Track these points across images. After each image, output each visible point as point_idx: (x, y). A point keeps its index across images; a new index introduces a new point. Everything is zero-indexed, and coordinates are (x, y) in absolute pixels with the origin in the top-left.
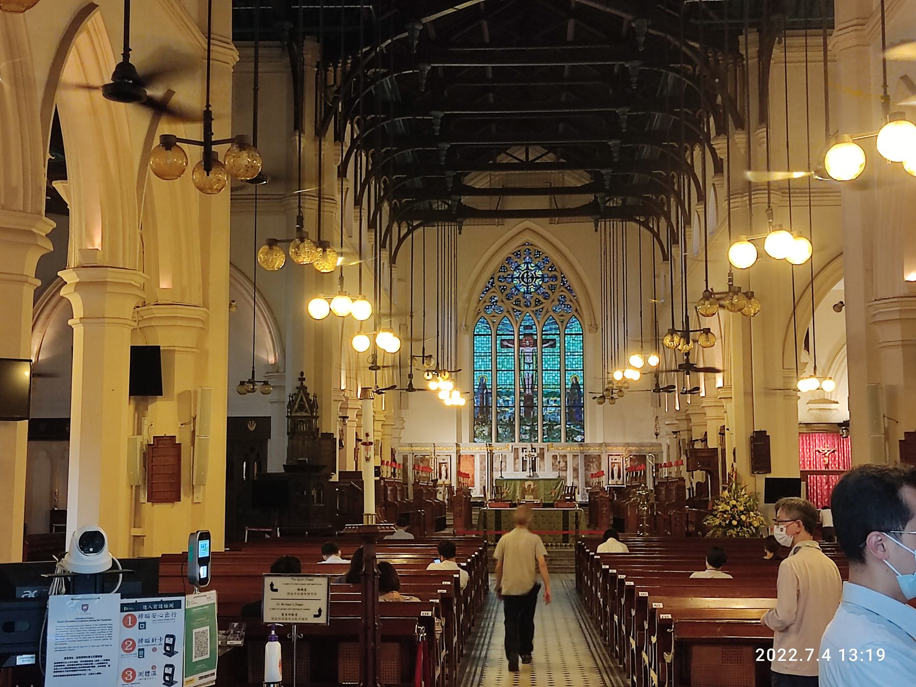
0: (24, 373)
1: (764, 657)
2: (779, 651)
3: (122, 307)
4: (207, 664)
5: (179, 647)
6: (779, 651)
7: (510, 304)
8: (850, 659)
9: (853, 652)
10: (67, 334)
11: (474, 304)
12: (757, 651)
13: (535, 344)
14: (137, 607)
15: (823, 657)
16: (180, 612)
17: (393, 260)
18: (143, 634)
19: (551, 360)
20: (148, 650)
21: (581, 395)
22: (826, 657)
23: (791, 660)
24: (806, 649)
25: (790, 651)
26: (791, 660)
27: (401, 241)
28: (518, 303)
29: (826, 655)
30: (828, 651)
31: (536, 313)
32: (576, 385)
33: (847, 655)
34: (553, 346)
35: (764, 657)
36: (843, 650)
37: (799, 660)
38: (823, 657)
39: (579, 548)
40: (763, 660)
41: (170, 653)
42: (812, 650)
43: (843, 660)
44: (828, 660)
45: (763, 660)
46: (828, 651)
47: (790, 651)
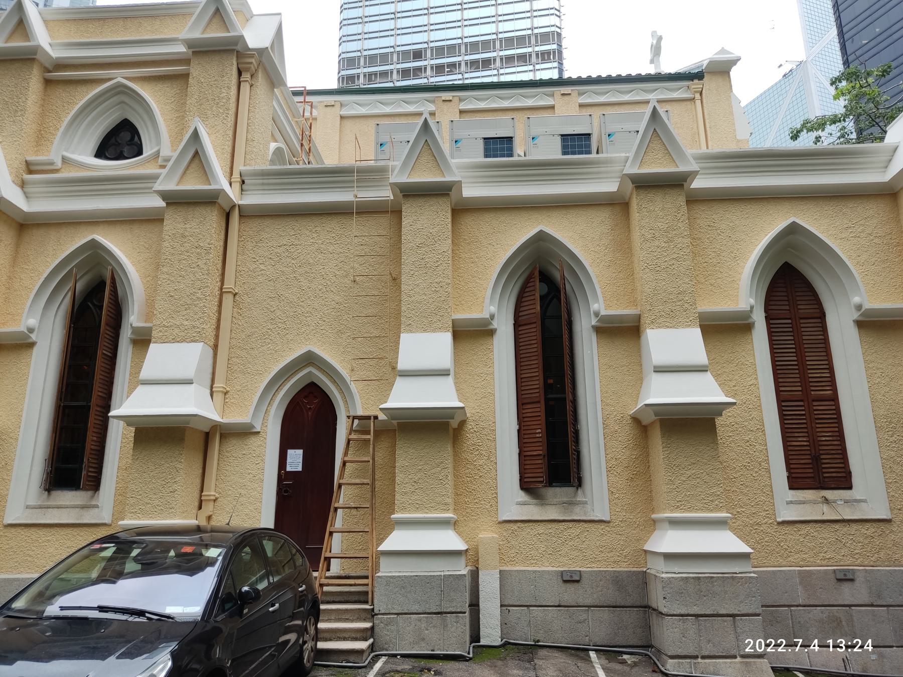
1: (754, 647)
2: (768, 642)
9: (841, 642)
12: (746, 642)
24: (795, 640)
25: (779, 642)
35: (754, 647)
37: (787, 650)
40: (753, 651)
42: (801, 640)
45: (753, 651)
47: (779, 642)
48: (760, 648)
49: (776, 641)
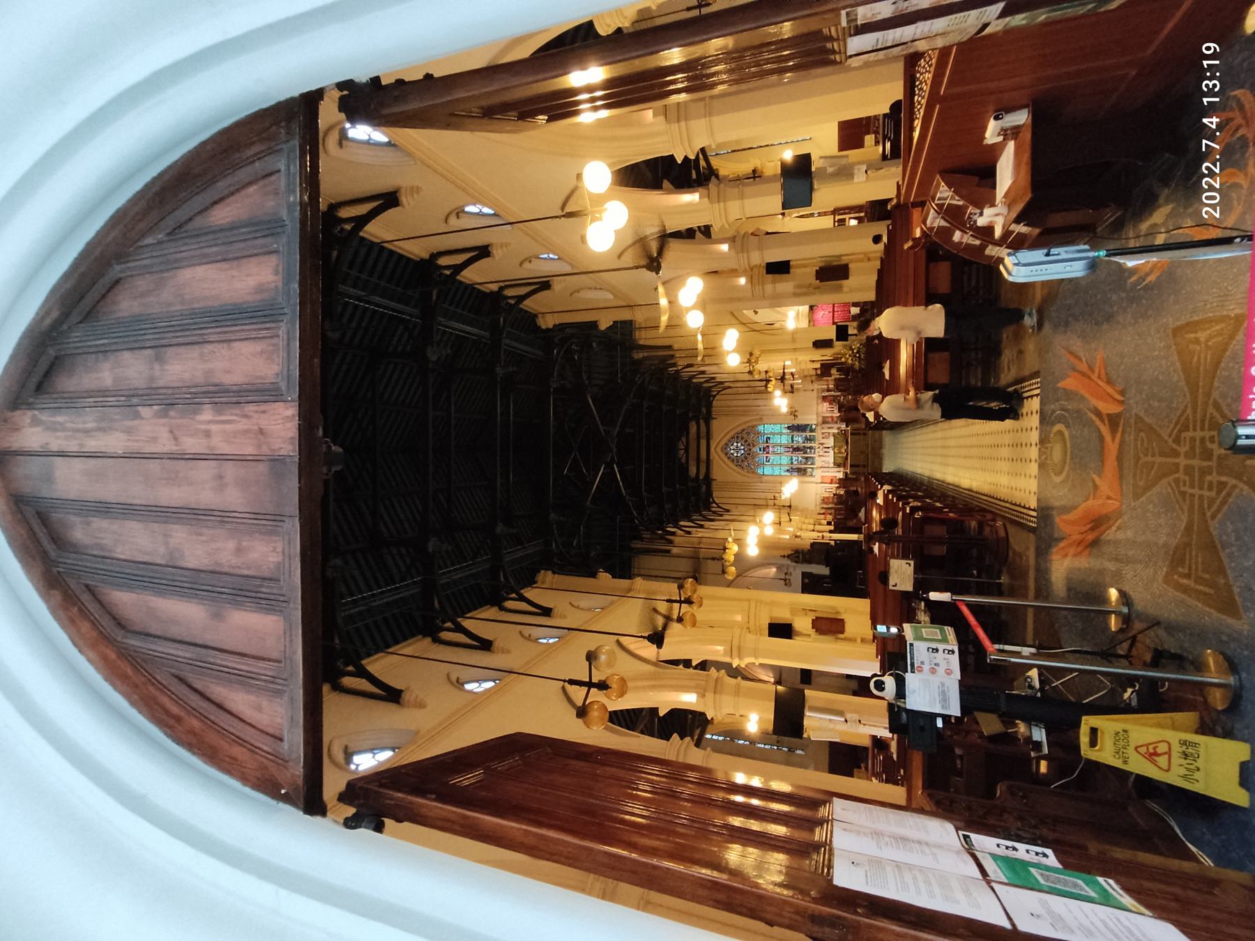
0: (779, 688)
1: (1213, 207)
3: (750, 640)
4: (942, 632)
5: (934, 645)
6: (1206, 187)
7: (749, 457)
8: (1216, 90)
10: (761, 665)
11: (750, 475)
12: (1206, 217)
13: (768, 446)
14: (912, 665)
15: (1214, 127)
16: (916, 644)
17: (728, 511)
18: (927, 663)
19: (776, 440)
20: (936, 661)
21: (793, 426)
22: (1214, 124)
23: (1217, 171)
24: (1204, 150)
25: (1206, 172)
26: (1217, 171)
27: (719, 507)
28: (749, 455)
29: (1212, 123)
30: (1205, 121)
31: (754, 446)
32: (788, 428)
33: (1211, 93)
34: (769, 438)
35: (1213, 207)
36: (1205, 100)
37: (1218, 160)
38: (1214, 127)
39: (871, 429)
40: (1218, 208)
41: (937, 650)
42: (1204, 141)
43: (1218, 99)
44: (1218, 120)
45: (1218, 208)
46: (1205, 121)
47: (1206, 172)
48: (1214, 198)
49: (1205, 176)
